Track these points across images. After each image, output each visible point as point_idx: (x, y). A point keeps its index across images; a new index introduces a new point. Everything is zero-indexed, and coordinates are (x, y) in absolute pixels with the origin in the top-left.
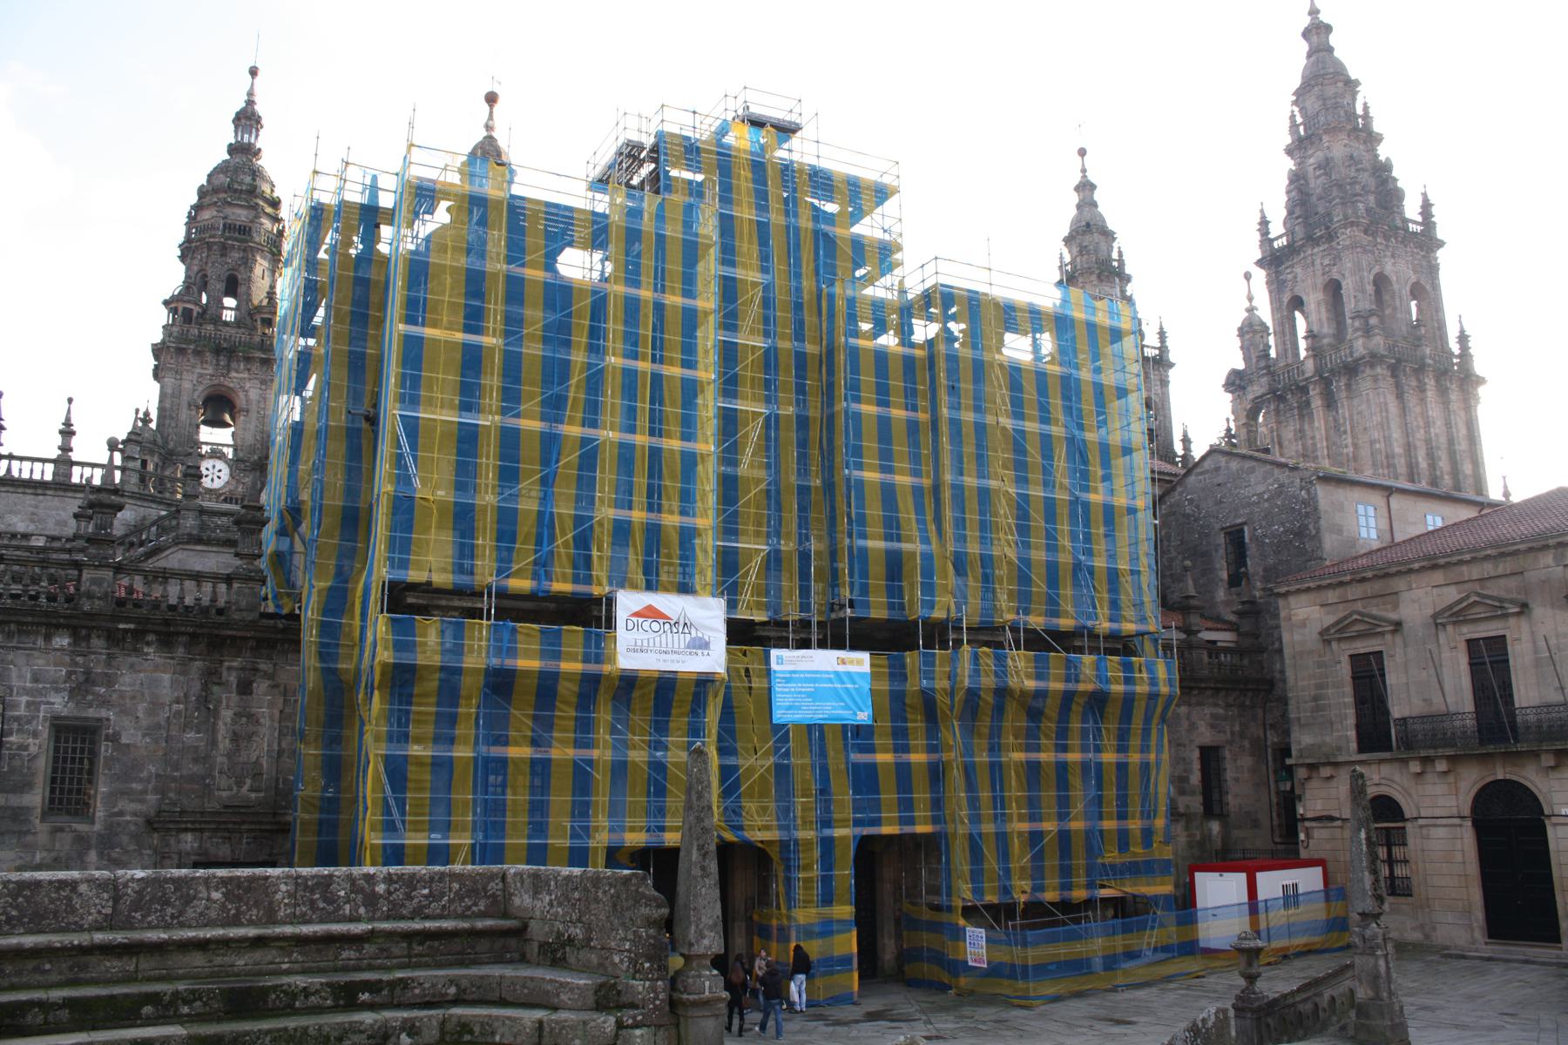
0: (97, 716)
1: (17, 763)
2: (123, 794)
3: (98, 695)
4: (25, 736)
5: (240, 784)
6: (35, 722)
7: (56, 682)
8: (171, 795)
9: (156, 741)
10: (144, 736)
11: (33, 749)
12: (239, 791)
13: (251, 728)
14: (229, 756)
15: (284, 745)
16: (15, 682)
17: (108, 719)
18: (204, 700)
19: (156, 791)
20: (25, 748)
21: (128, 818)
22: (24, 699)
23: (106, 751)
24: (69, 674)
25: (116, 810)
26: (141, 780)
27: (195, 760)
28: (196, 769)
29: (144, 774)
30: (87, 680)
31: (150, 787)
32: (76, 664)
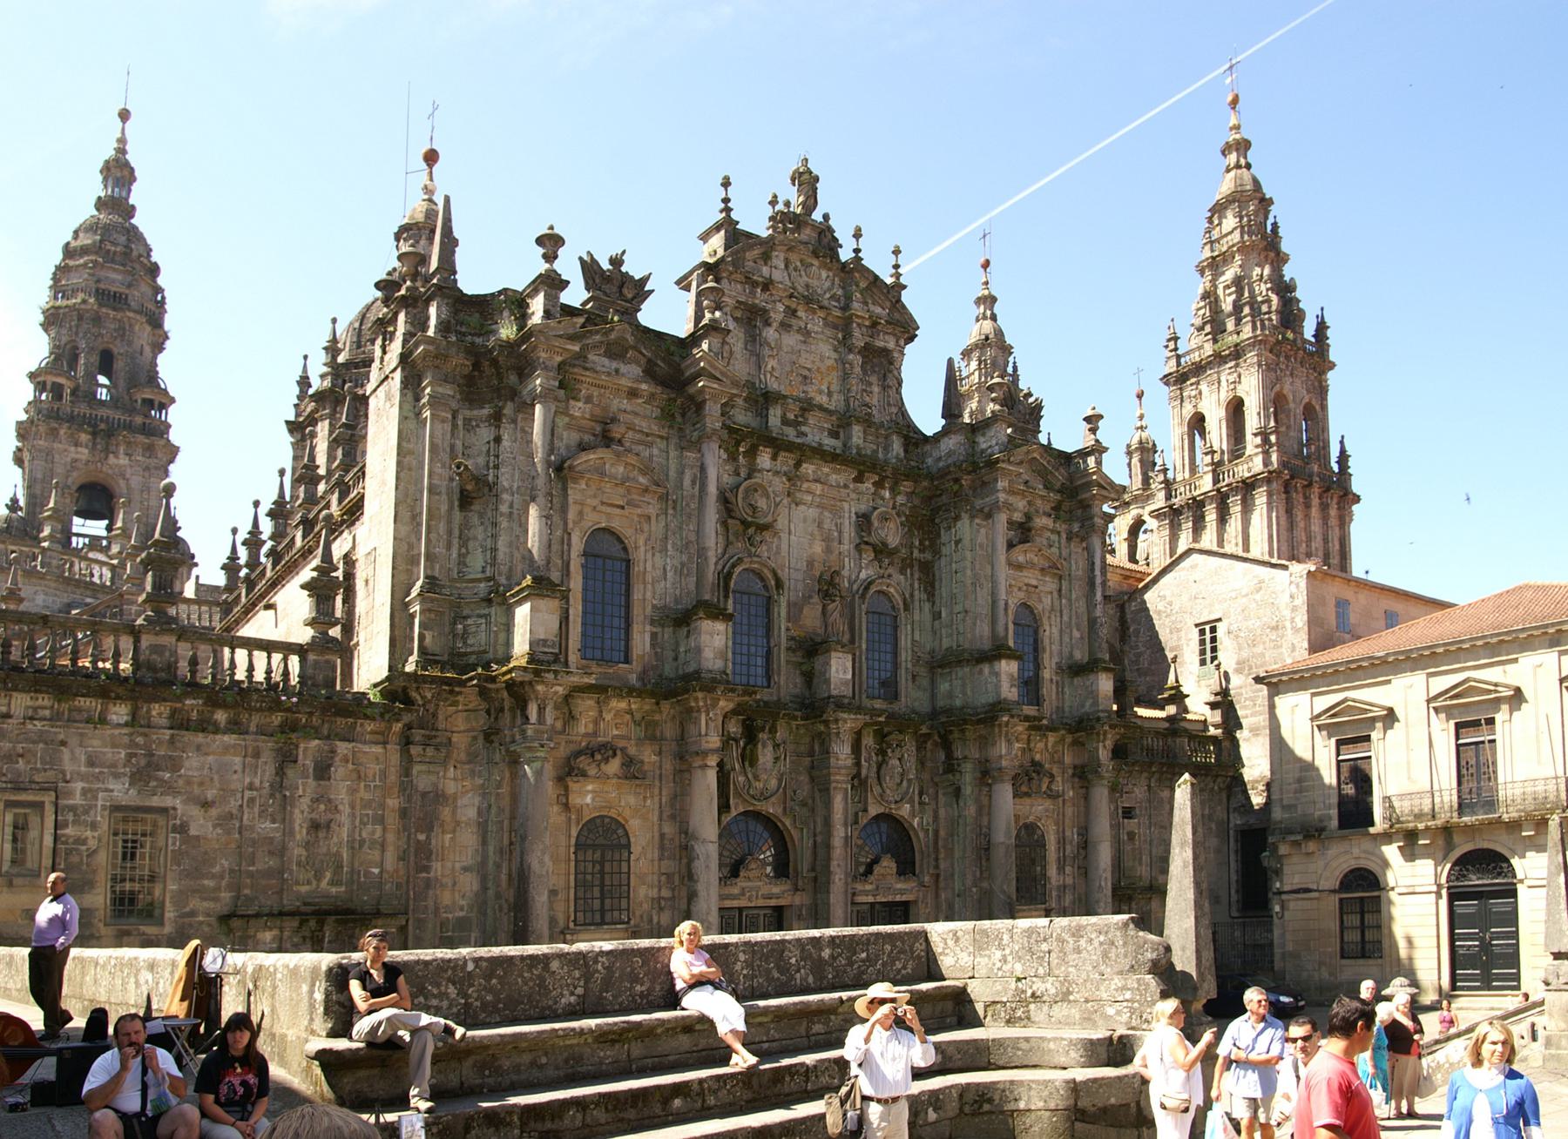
0: (163, 805)
1: (75, 859)
2: (194, 891)
3: (162, 780)
4: (83, 829)
5: (318, 876)
6: (92, 812)
7: (113, 765)
8: (247, 891)
9: (228, 832)
10: (215, 826)
11: (92, 844)
12: (318, 886)
13: (330, 816)
14: (307, 845)
15: (364, 835)
16: (68, 767)
17: (174, 809)
18: (279, 784)
19: (230, 887)
20: (84, 842)
21: (201, 918)
22: (79, 786)
23: (174, 844)
24: (130, 756)
25: (187, 909)
26: (213, 876)
27: (271, 853)
28: (273, 862)
29: (217, 869)
30: (149, 765)
31: (224, 883)
32: (137, 745)
